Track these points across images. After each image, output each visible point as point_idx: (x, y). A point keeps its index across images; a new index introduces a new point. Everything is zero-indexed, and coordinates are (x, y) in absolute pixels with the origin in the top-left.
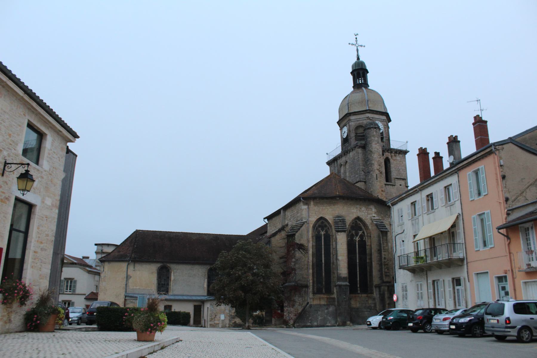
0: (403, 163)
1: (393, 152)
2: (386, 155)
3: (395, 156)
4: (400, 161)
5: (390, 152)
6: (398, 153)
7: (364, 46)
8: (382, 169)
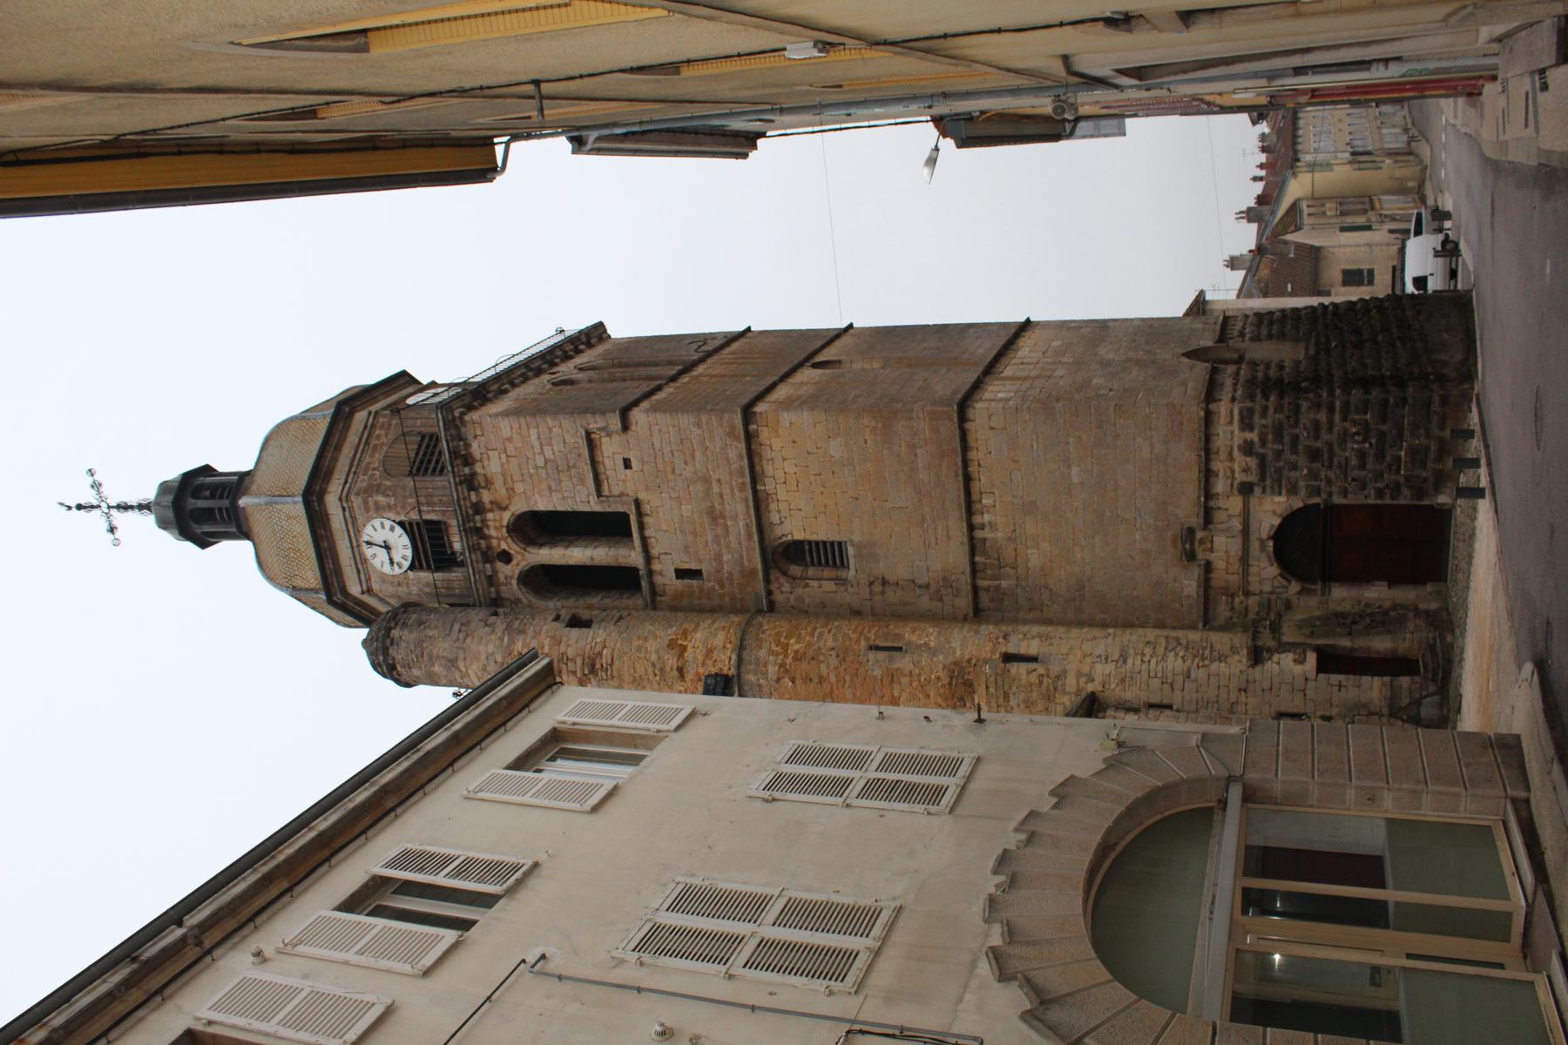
0: (510, 440)
1: (474, 498)
2: (505, 540)
3: (489, 483)
4: (503, 456)
5: (478, 518)
6: (467, 470)
7: (91, 472)
8: (573, 660)
